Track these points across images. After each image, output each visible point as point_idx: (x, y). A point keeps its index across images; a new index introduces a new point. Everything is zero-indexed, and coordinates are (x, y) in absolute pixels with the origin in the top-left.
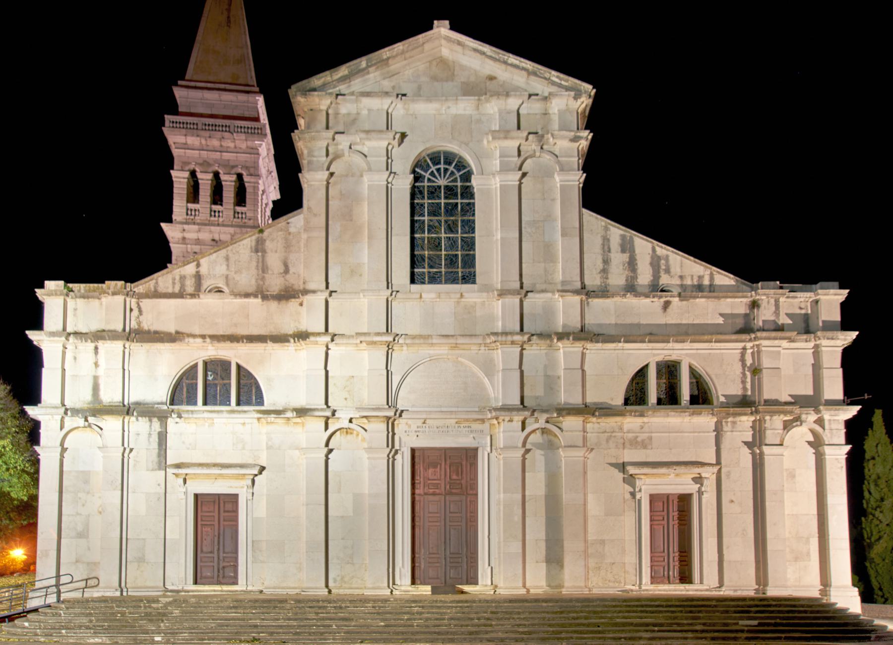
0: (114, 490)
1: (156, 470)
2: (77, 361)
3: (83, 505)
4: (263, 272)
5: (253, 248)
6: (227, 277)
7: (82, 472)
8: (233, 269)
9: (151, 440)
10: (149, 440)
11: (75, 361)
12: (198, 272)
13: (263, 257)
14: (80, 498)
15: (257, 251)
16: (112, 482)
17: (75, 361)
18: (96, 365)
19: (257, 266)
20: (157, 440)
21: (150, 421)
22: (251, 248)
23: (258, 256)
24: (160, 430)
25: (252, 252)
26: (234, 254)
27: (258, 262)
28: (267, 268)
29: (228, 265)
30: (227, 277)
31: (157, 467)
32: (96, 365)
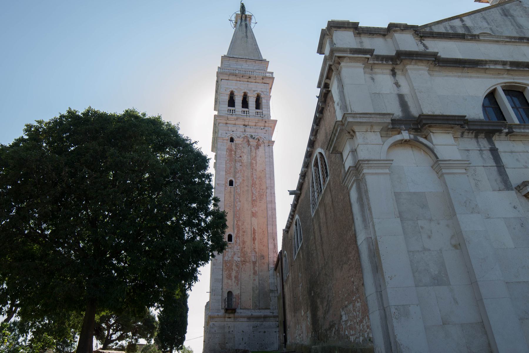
0: (472, 213)
1: (503, 190)
2: (375, 81)
3: (429, 237)
4: (519, 27)
5: (502, 14)
6: (491, 29)
7: (415, 193)
8: (493, 25)
9: (484, 156)
10: (482, 156)
11: (374, 81)
12: (463, 25)
13: (514, 19)
14: (422, 228)
15: (506, 16)
16: (465, 202)
17: (374, 81)
18: (397, 85)
19: (512, 24)
20: (491, 156)
21: (476, 137)
22: (500, 13)
23: (509, 18)
24: (490, 146)
25: (502, 16)
26: (489, 16)
27: (511, 22)
28: (521, 26)
29: (487, 22)
30: (491, 29)
31: (504, 187)
32: (397, 85)
